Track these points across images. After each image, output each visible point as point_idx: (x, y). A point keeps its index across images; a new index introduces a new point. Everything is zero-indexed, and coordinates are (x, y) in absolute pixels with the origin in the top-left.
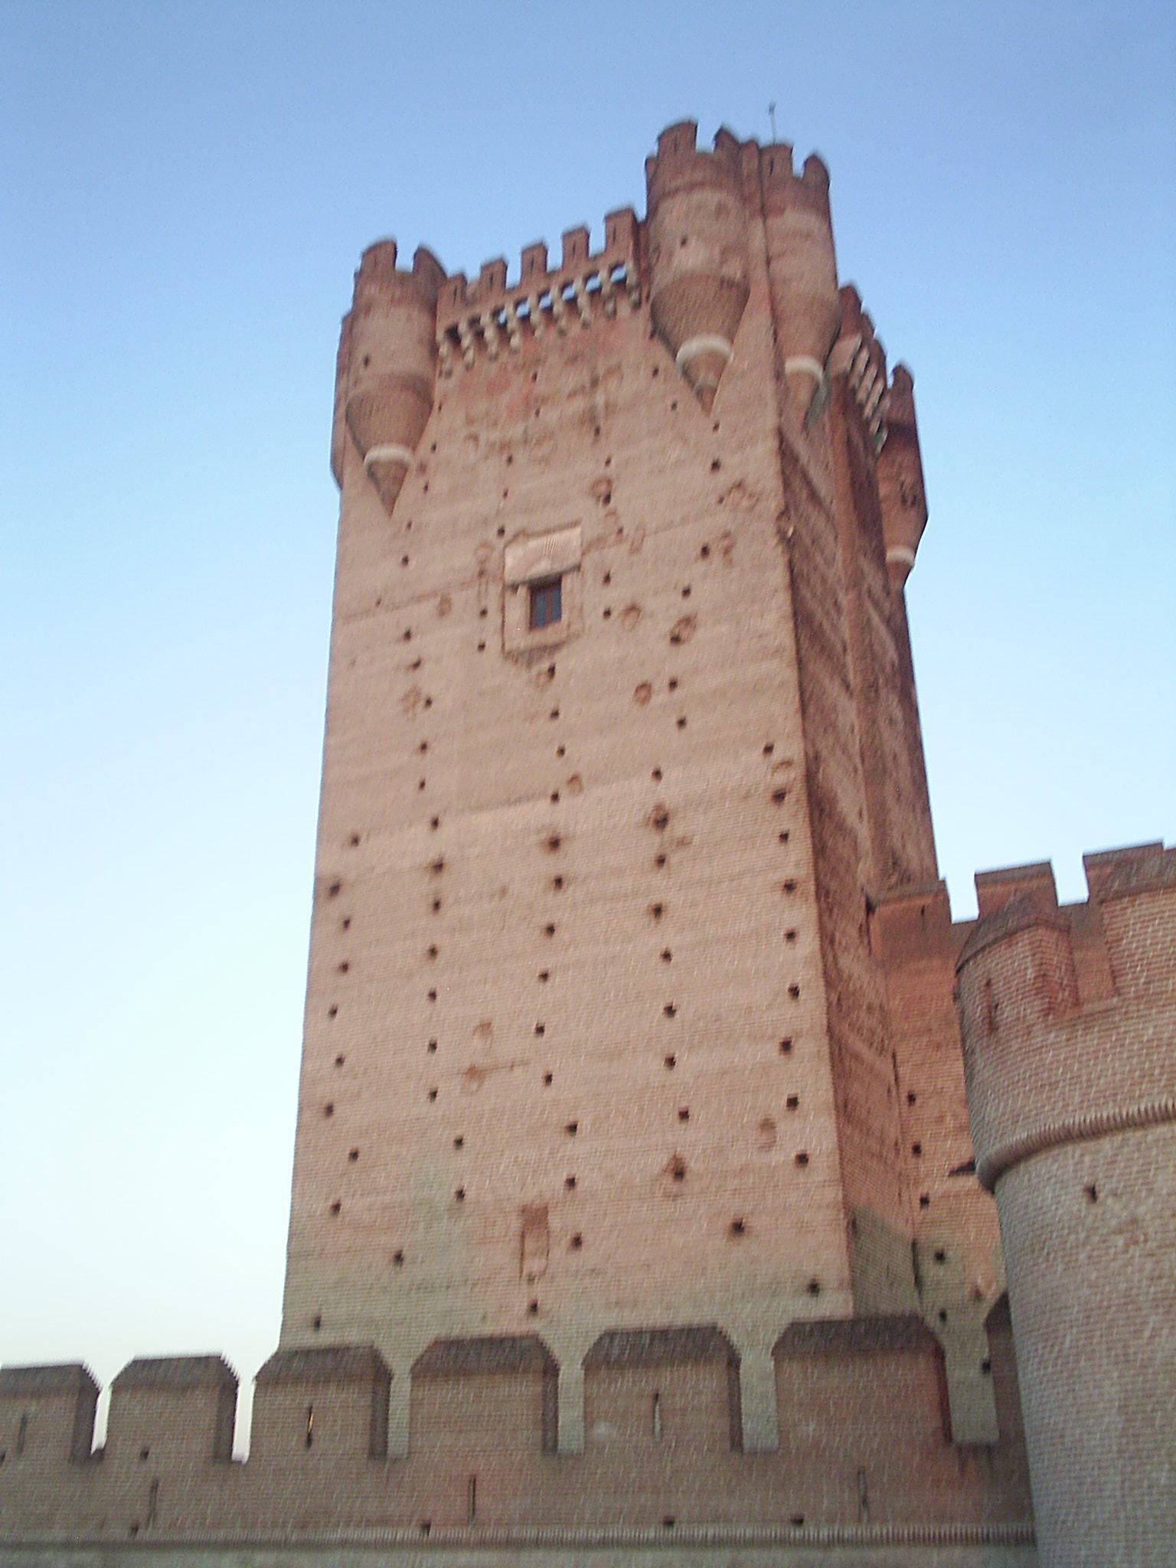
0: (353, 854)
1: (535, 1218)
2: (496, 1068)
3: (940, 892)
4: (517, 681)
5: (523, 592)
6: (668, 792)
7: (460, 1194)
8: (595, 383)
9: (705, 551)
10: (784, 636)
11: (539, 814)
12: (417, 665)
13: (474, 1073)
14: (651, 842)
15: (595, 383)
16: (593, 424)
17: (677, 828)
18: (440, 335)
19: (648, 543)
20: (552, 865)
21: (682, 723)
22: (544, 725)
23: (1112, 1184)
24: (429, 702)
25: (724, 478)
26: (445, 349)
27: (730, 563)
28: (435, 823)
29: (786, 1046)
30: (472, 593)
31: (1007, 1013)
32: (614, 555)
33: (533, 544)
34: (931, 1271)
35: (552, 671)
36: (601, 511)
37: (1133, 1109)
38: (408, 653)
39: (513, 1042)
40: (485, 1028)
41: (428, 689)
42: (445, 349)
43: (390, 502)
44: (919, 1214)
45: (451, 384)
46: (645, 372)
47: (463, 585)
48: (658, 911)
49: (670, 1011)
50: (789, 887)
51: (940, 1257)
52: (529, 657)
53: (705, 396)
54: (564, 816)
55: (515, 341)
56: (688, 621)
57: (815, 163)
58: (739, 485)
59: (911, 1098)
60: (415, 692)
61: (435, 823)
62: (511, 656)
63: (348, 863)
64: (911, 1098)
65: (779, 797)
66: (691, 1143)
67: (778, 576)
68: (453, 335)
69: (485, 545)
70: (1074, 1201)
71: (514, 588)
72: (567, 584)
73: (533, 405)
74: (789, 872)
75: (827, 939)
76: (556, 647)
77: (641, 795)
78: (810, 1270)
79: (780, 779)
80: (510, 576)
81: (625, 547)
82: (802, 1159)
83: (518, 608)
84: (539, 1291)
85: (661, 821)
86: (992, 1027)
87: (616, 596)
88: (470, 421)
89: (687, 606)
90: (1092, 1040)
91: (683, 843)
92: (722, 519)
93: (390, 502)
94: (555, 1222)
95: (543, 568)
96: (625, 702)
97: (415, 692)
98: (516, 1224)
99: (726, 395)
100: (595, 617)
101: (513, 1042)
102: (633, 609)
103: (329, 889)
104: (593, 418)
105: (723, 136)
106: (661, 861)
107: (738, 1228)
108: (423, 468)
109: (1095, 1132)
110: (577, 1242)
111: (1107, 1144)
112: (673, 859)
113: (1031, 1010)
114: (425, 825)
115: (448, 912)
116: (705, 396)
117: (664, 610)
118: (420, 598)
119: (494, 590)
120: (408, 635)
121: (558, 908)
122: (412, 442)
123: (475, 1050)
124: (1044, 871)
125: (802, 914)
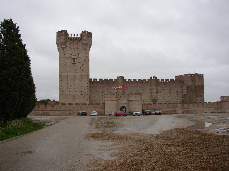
0: (62, 74)
4: (73, 65)
6: (82, 74)
11: (74, 74)
14: (80, 77)
16: (78, 49)
22: (74, 68)
25: (86, 56)
30: (69, 58)
38: (65, 61)
39: (72, 87)
40: (71, 86)
43: (63, 50)
48: (81, 81)
52: (74, 64)
54: (75, 74)
63: (61, 74)
66: (82, 93)
68: (68, 39)
78: (87, 99)
84: (74, 99)
87: (79, 61)
93: (63, 50)
95: (74, 58)
96: (79, 68)
99: (86, 50)
100: (78, 63)
101: (72, 87)
103: (60, 76)
105: (88, 32)
114: (66, 73)
116: (85, 50)
123: (70, 87)
125: (88, 82)
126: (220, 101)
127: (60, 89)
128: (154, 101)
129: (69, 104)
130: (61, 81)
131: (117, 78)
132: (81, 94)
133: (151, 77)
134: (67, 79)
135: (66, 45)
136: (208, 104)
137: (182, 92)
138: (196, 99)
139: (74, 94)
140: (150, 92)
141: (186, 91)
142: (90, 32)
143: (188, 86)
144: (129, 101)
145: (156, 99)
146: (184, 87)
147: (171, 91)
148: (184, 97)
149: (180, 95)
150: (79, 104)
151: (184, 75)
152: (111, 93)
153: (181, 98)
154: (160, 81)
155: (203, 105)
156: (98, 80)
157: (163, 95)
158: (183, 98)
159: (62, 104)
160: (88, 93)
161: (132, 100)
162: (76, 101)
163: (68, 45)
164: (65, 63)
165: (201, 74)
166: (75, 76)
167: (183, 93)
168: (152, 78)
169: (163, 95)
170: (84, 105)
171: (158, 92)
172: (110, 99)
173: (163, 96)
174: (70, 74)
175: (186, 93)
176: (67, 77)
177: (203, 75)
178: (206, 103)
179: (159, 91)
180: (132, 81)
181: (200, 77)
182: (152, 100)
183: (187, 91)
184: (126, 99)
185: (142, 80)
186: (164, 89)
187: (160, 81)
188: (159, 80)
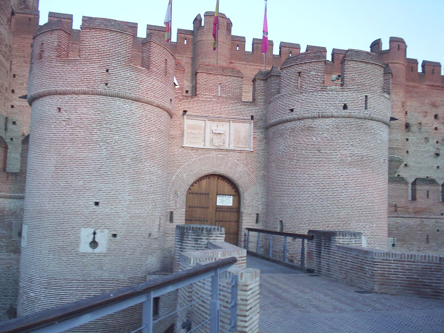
23: (65, 109)
31: (46, 54)
34: (10, 126)
37: (76, 89)
44: (10, 110)
51: (14, 123)
59: (14, 76)
64: (14, 76)
70: (54, 111)
86: (41, 57)
90: (69, 68)
109: (64, 93)
111: (66, 97)
113: (54, 54)
145: (401, 162)
157: (432, 142)
161: (299, 111)
169: (432, 142)
173: (431, 148)
188: (415, 62)
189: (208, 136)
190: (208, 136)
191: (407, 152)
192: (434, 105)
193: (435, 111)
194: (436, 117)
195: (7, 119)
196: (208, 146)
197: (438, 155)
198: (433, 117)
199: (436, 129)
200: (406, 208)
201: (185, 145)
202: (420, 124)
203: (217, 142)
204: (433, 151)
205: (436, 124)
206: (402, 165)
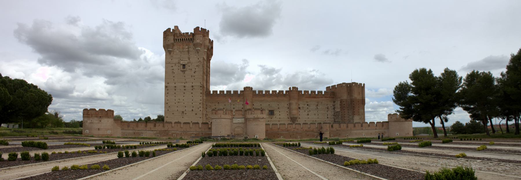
0: (168, 84)
1: (183, 112)
2: (180, 102)
3: (210, 91)
4: (182, 73)
5: (182, 65)
6: (193, 85)
7: (178, 110)
8: (188, 48)
9: (197, 66)
10: (202, 75)
12: (173, 69)
13: (178, 102)
15: (188, 48)
17: (194, 87)
18: (175, 39)
19: (193, 64)
20: (184, 88)
21: (194, 79)
24: (174, 73)
26: (175, 40)
27: (199, 68)
28: (175, 83)
29: (200, 103)
30: (178, 64)
32: (190, 64)
33: (183, 61)
35: (185, 73)
36: (189, 60)
41: (174, 72)
42: (175, 40)
43: (170, 54)
45: (176, 43)
46: (193, 49)
47: (177, 63)
48: (192, 93)
49: (192, 100)
50: (201, 93)
52: (183, 71)
53: (198, 52)
54: (186, 85)
55: (182, 42)
56: (195, 71)
57: (208, 31)
58: (200, 61)
60: (173, 72)
61: (175, 83)
62: (181, 71)
63: (168, 85)
65: (201, 87)
66: (193, 109)
67: (202, 70)
68: (176, 39)
69: (179, 60)
71: (181, 65)
72: (186, 65)
73: (183, 48)
74: (201, 92)
75: (203, 97)
76: (185, 71)
77: (191, 84)
78: (200, 117)
79: (201, 85)
80: (181, 64)
81: (191, 64)
82: (200, 110)
83: (182, 67)
84: (183, 116)
85: (193, 87)
87: (190, 68)
88: (178, 48)
89: (195, 70)
91: (194, 89)
92: (198, 64)
93: (170, 54)
94: (184, 112)
95: (184, 64)
97: (173, 72)
98: (181, 112)
99: (200, 53)
100: (188, 69)
102: (191, 69)
103: (166, 87)
104: (188, 51)
106: (192, 90)
107: (196, 114)
108: (173, 51)
110: (186, 114)
112: (193, 89)
115: (176, 91)
116: (198, 52)
117: (194, 70)
118: (173, 64)
119: (180, 65)
120: (172, 67)
121: (185, 92)
122: (172, 49)
124: (217, 91)
126: (387, 121)
127: (166, 103)
128: (293, 120)
129: (175, 123)
130: (167, 94)
131: (243, 90)
132: (192, 110)
133: (290, 88)
134: (174, 91)
135: (173, 47)
136: (369, 126)
137: (334, 108)
138: (353, 117)
139: (184, 110)
140: (288, 108)
141: (339, 106)
142: (206, 30)
143: (341, 99)
144: (246, 119)
146: (337, 102)
147: (318, 107)
148: (336, 114)
149: (331, 113)
150: (189, 123)
151: (337, 85)
152: (235, 109)
153: (333, 117)
154: (303, 93)
155: (362, 126)
156: (218, 93)
157: (307, 111)
158: (336, 116)
159: (167, 122)
160: (201, 109)
162: (186, 119)
163: (175, 47)
164: (172, 71)
165: (361, 84)
166: (185, 87)
167: (335, 110)
168: (292, 89)
169: (307, 111)
170: (185, 124)
171: (299, 108)
172: (216, 116)
173: (306, 113)
174: (179, 84)
175: (339, 110)
176: (174, 88)
177: (364, 84)
178: (367, 123)
179: (301, 106)
180: (264, 93)
181: (361, 88)
182: (291, 118)
183: (340, 107)
184: (244, 116)
185: (278, 92)
186: (309, 104)
187: (303, 93)
188: (301, 91)
189: (237, 121)
190: (237, 121)
191: (300, 115)
192: (307, 102)
193: (307, 104)
194: (308, 105)
195: (206, 114)
196: (237, 122)
197: (308, 115)
198: (307, 105)
199: (308, 108)
200: (285, 130)
201: (234, 122)
202: (303, 107)
203: (239, 122)
204: (307, 114)
205: (307, 107)
206: (298, 118)
